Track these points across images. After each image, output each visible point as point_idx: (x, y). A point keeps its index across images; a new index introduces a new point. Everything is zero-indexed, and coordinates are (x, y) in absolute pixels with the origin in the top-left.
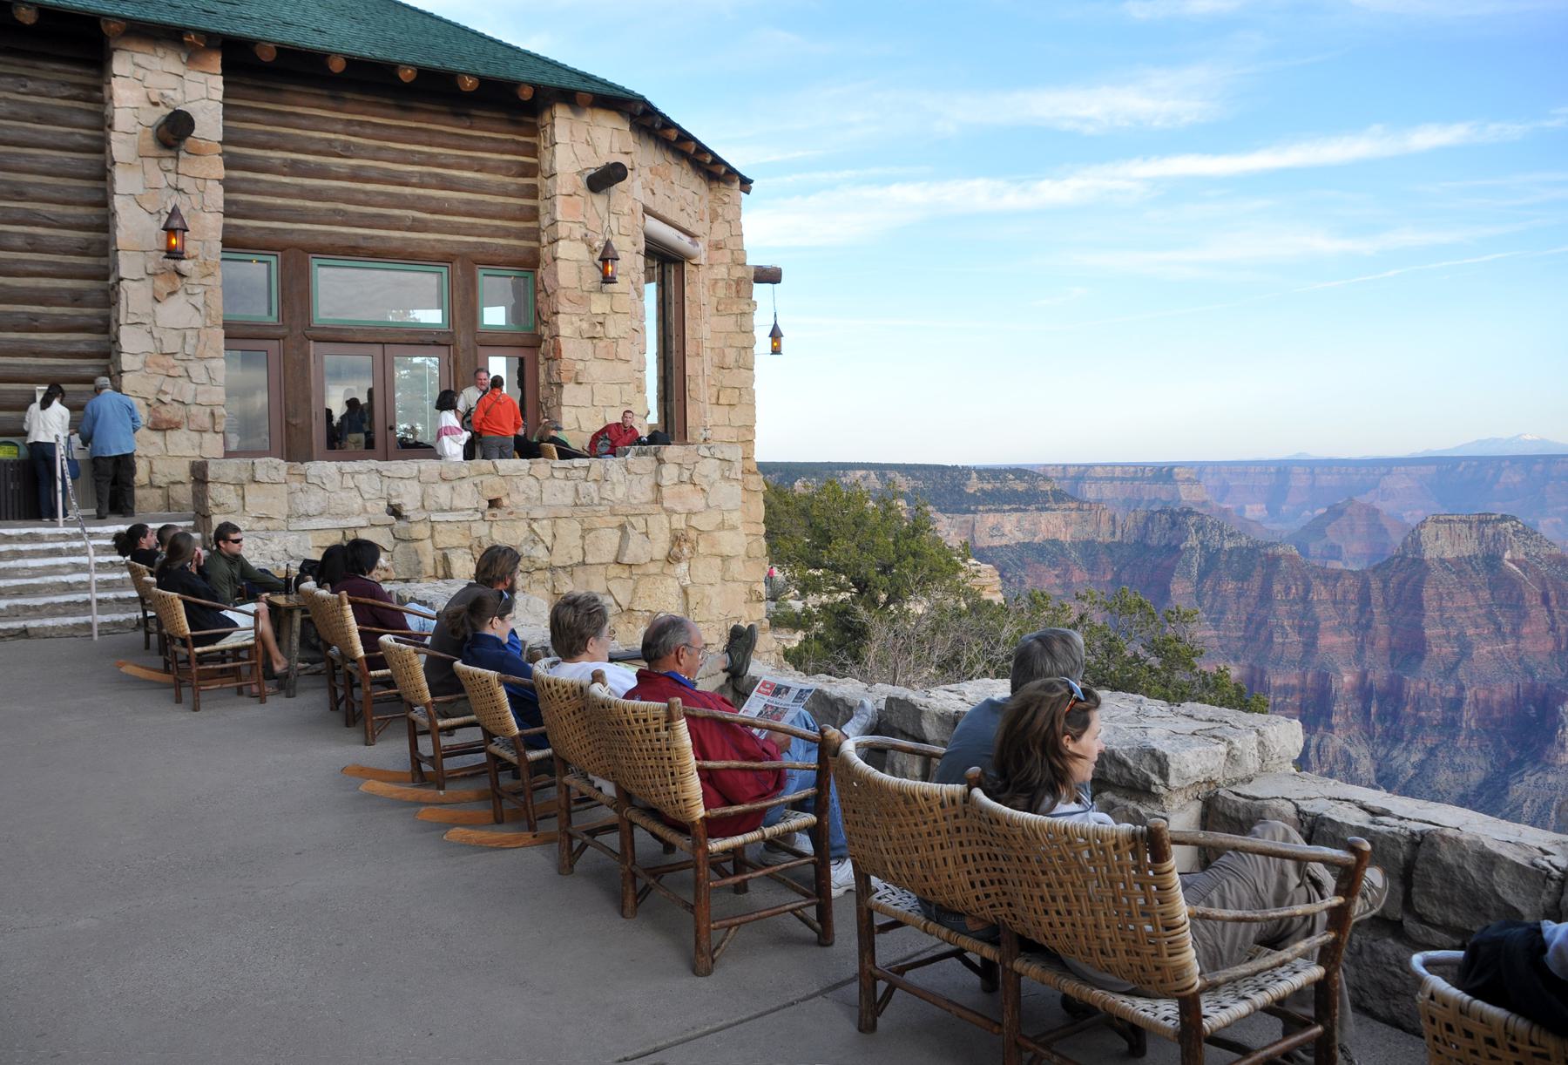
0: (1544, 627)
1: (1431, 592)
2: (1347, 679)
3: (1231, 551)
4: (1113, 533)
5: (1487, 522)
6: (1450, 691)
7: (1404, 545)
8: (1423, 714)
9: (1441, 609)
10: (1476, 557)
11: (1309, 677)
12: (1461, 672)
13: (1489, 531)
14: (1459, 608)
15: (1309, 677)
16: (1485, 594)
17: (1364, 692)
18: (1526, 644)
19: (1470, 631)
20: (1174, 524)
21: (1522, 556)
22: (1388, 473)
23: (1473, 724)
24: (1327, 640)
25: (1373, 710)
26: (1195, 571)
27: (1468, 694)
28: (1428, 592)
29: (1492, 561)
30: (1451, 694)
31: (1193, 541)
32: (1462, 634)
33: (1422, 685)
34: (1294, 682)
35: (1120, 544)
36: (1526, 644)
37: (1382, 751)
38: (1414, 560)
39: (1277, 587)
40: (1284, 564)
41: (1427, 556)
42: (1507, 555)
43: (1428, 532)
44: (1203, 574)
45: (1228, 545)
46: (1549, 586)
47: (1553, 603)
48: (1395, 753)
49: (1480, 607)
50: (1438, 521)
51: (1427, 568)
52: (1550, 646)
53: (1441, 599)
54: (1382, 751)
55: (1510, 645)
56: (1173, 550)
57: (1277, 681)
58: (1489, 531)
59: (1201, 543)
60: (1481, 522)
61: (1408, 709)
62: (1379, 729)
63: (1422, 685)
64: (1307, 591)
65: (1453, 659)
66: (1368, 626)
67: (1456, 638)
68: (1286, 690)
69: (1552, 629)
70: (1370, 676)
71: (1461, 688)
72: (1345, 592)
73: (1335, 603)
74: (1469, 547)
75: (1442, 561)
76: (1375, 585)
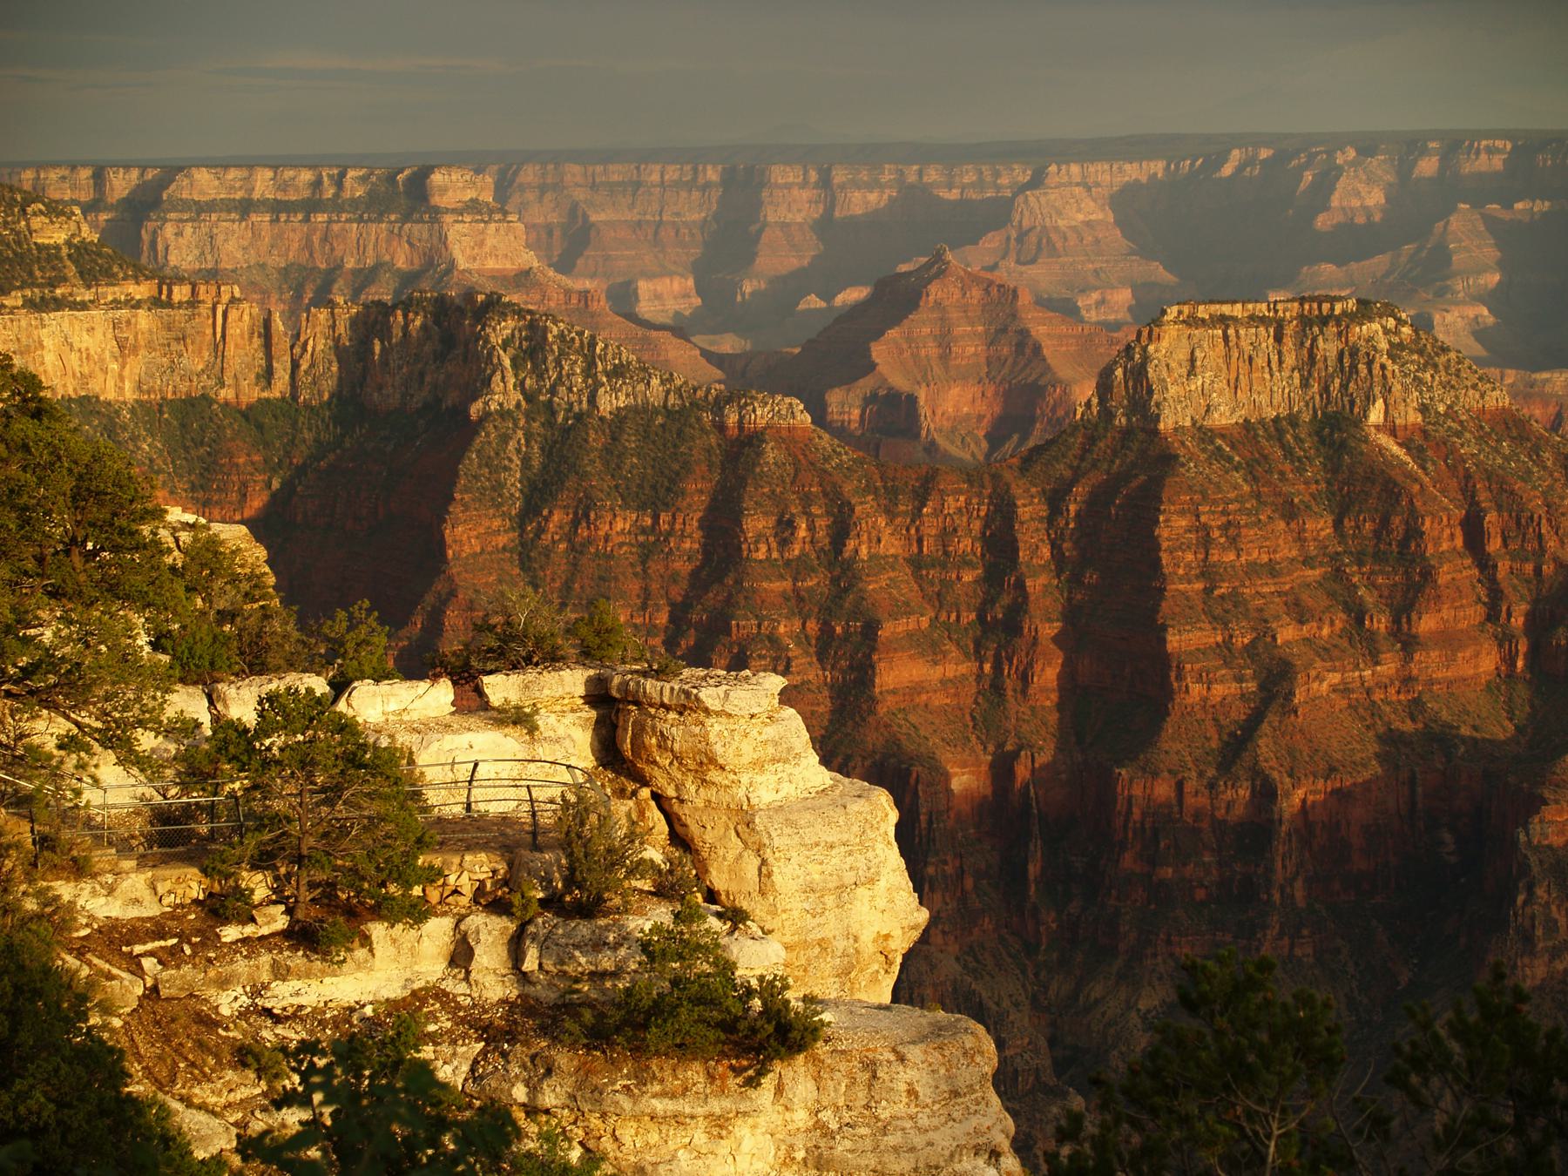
0: (1473, 614)
3: (620, 416)
5: (1324, 321)
7: (1104, 387)
9: (1208, 573)
10: (1293, 420)
12: (1265, 747)
13: (1328, 347)
14: (1253, 570)
16: (1320, 526)
18: (1429, 663)
19: (1287, 633)
20: (448, 341)
21: (1415, 418)
22: (1037, 181)
25: (1033, 870)
26: (513, 481)
28: (1173, 526)
29: (1335, 429)
31: (504, 393)
32: (1264, 633)
33: (1163, 790)
36: (1429, 663)
39: (756, 524)
40: (771, 454)
41: (1166, 424)
42: (1376, 415)
43: (1169, 347)
44: (538, 496)
45: (608, 403)
46: (1483, 497)
47: (1494, 545)
48: (1097, 990)
49: (1308, 562)
50: (1192, 322)
51: (1168, 460)
52: (1488, 662)
53: (1206, 543)
55: (1389, 666)
58: (1328, 347)
59: (530, 397)
60: (1305, 321)
61: (1128, 861)
62: (1050, 919)
64: (841, 530)
65: (1239, 713)
66: (1012, 625)
67: (1250, 649)
69: (1492, 615)
70: (1022, 771)
72: (946, 535)
73: (917, 563)
74: (1275, 392)
75: (1205, 435)
76: (1030, 509)
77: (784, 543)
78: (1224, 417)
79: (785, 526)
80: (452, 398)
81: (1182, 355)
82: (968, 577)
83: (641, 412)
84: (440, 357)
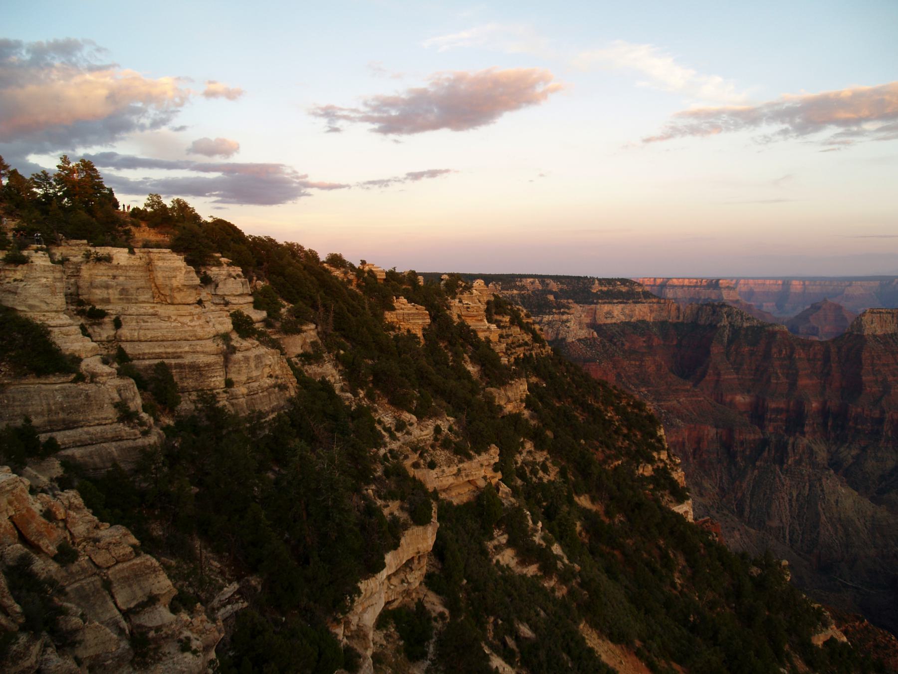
1: (868, 354)
2: (814, 405)
4: (678, 317)
6: (876, 414)
7: (852, 326)
8: (859, 427)
11: (792, 403)
15: (792, 403)
17: (824, 412)
19: (890, 378)
20: (714, 312)
22: (850, 285)
23: (889, 433)
24: (803, 382)
25: (829, 424)
26: (726, 339)
27: (887, 415)
28: (865, 355)
30: (877, 415)
31: (725, 322)
33: (859, 410)
34: (782, 406)
35: (682, 323)
37: (834, 448)
38: (858, 335)
39: (774, 350)
40: (778, 336)
41: (866, 333)
43: (866, 318)
44: (730, 342)
45: (745, 325)
48: (842, 449)
50: (872, 313)
54: (834, 448)
56: (713, 327)
57: (773, 405)
59: (730, 323)
61: (850, 423)
63: (859, 410)
68: (778, 411)
70: (828, 404)
71: (883, 412)
75: (875, 336)
77: (780, 354)
78: (879, 332)
79: (780, 352)
80: (714, 323)
81: (870, 319)
82: (819, 363)
83: (751, 328)
84: (712, 315)
